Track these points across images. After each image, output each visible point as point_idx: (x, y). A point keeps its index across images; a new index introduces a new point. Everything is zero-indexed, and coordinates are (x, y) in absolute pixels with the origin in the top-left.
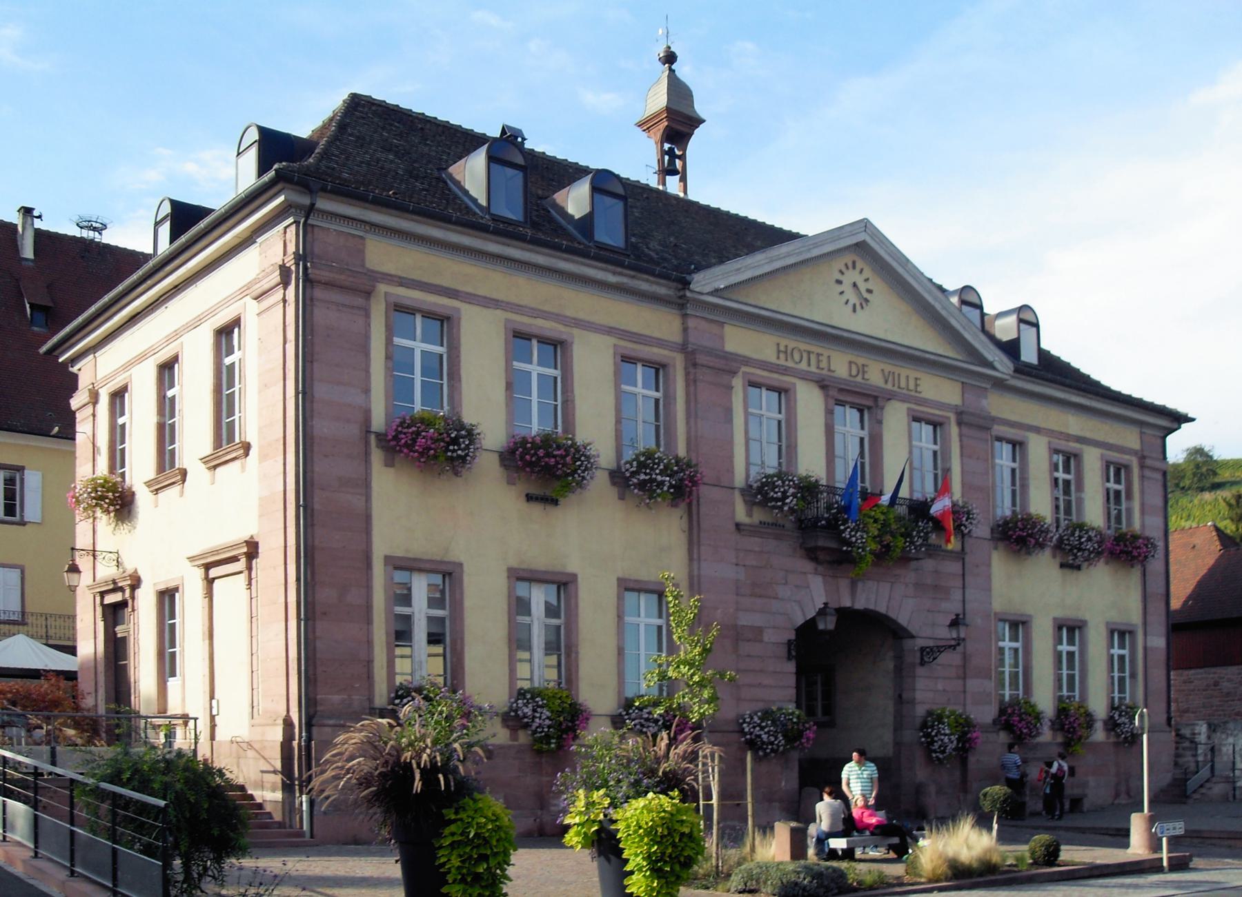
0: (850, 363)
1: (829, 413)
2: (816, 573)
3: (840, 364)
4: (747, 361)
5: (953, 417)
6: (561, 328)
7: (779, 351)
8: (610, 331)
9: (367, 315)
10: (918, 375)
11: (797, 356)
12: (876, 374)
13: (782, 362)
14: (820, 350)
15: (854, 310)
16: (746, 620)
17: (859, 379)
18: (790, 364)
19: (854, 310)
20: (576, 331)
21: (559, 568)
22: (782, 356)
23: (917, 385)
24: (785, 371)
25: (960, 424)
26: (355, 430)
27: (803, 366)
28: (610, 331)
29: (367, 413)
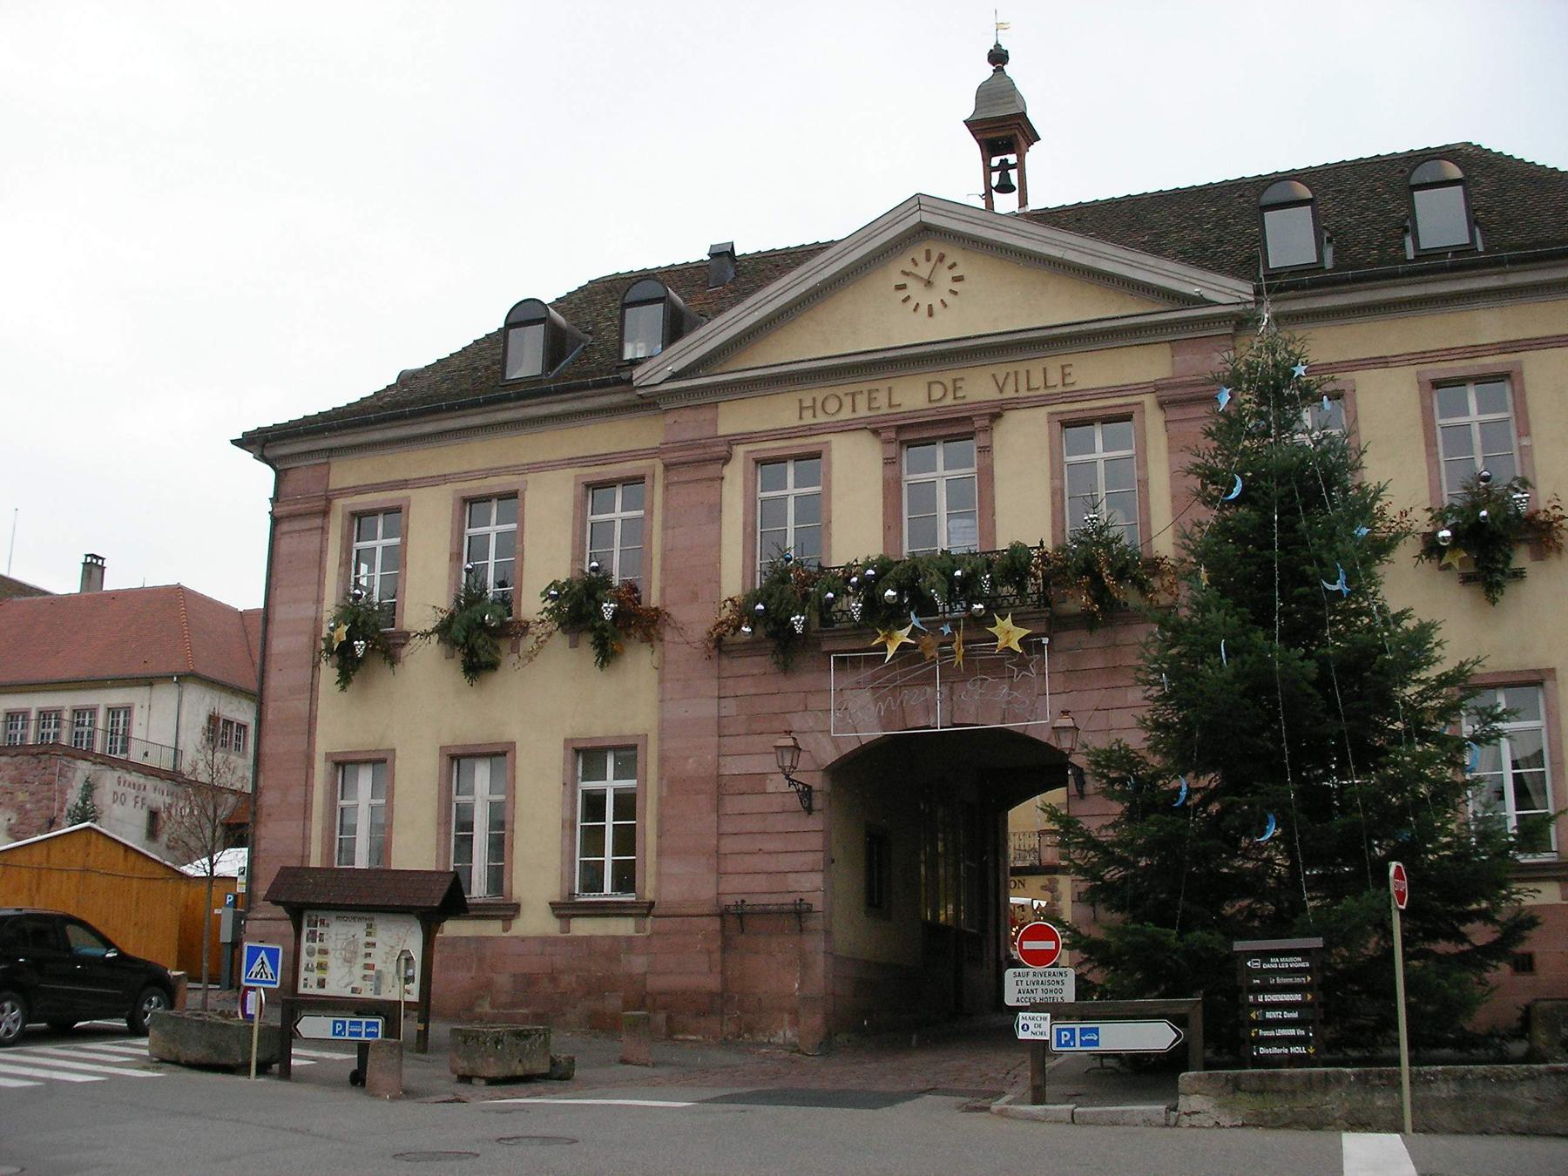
0: (930, 384)
1: (889, 462)
2: (859, 686)
3: (911, 396)
4: (747, 438)
5: (1149, 400)
6: (514, 479)
7: (801, 409)
8: (570, 462)
9: (324, 530)
10: (1064, 360)
11: (832, 406)
12: (979, 386)
13: (808, 419)
14: (873, 386)
15: (931, 315)
16: (733, 767)
17: (949, 401)
18: (822, 418)
19: (931, 315)
20: (530, 477)
21: (495, 738)
22: (808, 414)
23: (1064, 376)
24: (811, 430)
25: (1162, 405)
26: (305, 640)
27: (846, 414)
28: (570, 462)
29: (317, 621)
